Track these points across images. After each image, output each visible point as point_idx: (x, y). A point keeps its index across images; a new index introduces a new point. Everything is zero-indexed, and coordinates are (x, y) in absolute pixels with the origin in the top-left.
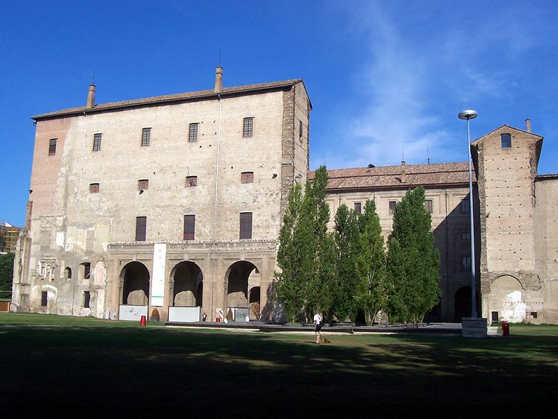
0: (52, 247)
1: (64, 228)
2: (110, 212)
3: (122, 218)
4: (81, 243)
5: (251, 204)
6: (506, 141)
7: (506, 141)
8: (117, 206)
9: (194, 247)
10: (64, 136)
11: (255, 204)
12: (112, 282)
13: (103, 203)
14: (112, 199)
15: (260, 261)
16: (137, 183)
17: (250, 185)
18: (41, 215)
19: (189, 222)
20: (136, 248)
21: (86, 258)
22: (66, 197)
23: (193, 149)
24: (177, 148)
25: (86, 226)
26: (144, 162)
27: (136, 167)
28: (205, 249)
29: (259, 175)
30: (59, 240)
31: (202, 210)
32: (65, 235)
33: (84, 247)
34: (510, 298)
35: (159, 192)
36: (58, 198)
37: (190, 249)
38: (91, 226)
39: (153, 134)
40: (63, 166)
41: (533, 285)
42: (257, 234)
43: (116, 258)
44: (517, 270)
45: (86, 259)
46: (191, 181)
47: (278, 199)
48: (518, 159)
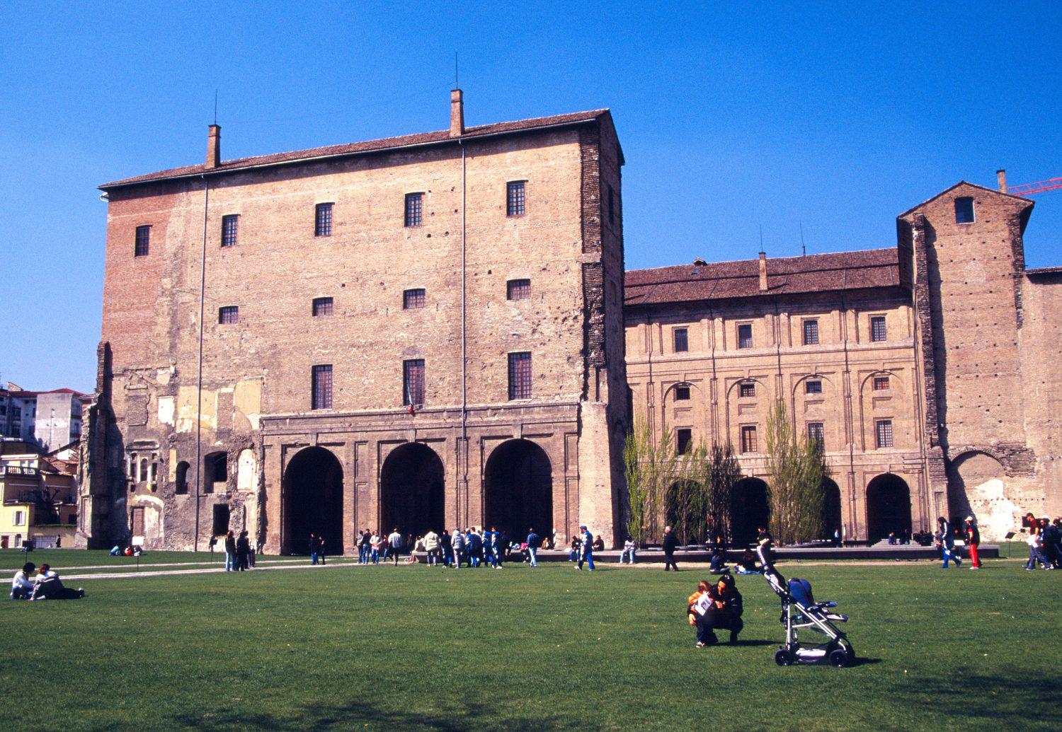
1: (173, 390)
2: (260, 358)
3: (286, 369)
5: (529, 337)
6: (964, 210)
7: (964, 210)
9: (426, 418)
10: (165, 221)
11: (536, 336)
12: (270, 486)
13: (247, 341)
15: (549, 439)
16: (310, 305)
17: (526, 304)
18: (125, 366)
19: (413, 369)
20: (316, 423)
21: (219, 443)
22: (174, 333)
23: (416, 239)
24: (385, 240)
25: (214, 385)
26: (323, 266)
27: (309, 275)
29: (541, 285)
30: (164, 411)
31: (437, 350)
32: (175, 402)
33: (215, 425)
34: (983, 491)
35: (354, 319)
36: (158, 335)
37: (418, 420)
38: (226, 385)
39: (337, 214)
40: (165, 277)
41: (1025, 468)
42: (541, 392)
43: (275, 442)
44: (993, 441)
46: (412, 297)
47: (579, 326)
48: (989, 241)
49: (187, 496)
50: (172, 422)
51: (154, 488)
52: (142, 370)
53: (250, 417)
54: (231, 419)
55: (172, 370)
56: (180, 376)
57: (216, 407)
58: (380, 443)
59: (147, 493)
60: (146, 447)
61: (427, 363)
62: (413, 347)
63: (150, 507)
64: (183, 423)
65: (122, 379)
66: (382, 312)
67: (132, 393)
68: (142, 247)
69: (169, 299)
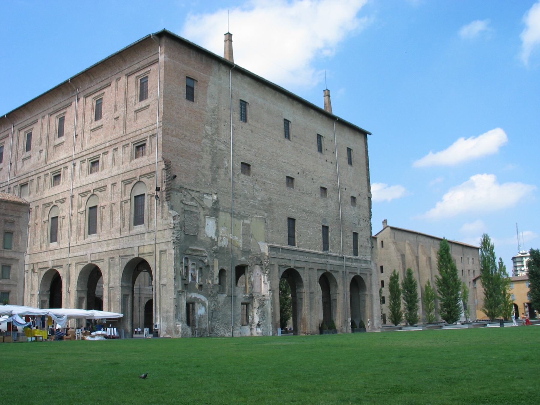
0: (201, 238)
1: (215, 211)
4: (237, 238)
8: (270, 199)
13: (257, 191)
14: (265, 190)
21: (243, 258)
22: (216, 168)
28: (338, 262)
30: (210, 228)
32: (217, 222)
33: (240, 243)
38: (246, 217)
45: (242, 260)
49: (225, 295)
50: (214, 237)
51: (201, 286)
52: (193, 191)
53: (259, 243)
54: (250, 244)
55: (215, 197)
56: (220, 203)
57: (241, 233)
58: (318, 270)
59: (196, 291)
60: (194, 253)
61: (330, 229)
62: (325, 219)
63: (199, 303)
64: (222, 240)
65: (179, 194)
66: (314, 196)
67: (187, 208)
68: (190, 95)
69: (210, 142)
